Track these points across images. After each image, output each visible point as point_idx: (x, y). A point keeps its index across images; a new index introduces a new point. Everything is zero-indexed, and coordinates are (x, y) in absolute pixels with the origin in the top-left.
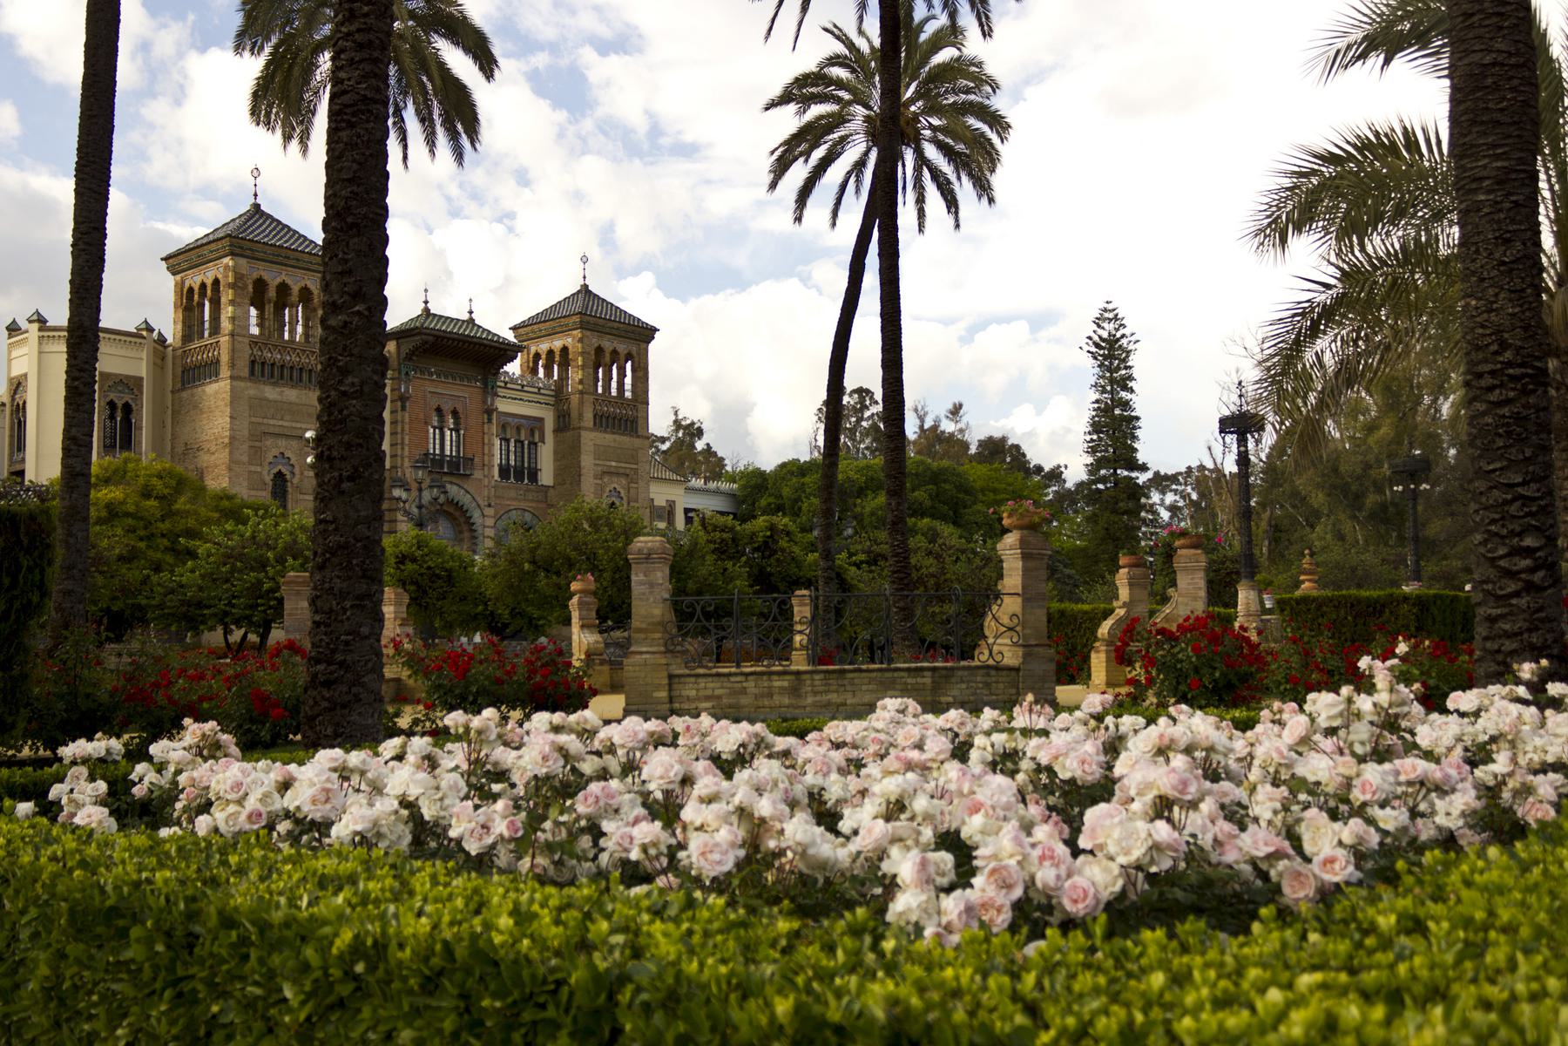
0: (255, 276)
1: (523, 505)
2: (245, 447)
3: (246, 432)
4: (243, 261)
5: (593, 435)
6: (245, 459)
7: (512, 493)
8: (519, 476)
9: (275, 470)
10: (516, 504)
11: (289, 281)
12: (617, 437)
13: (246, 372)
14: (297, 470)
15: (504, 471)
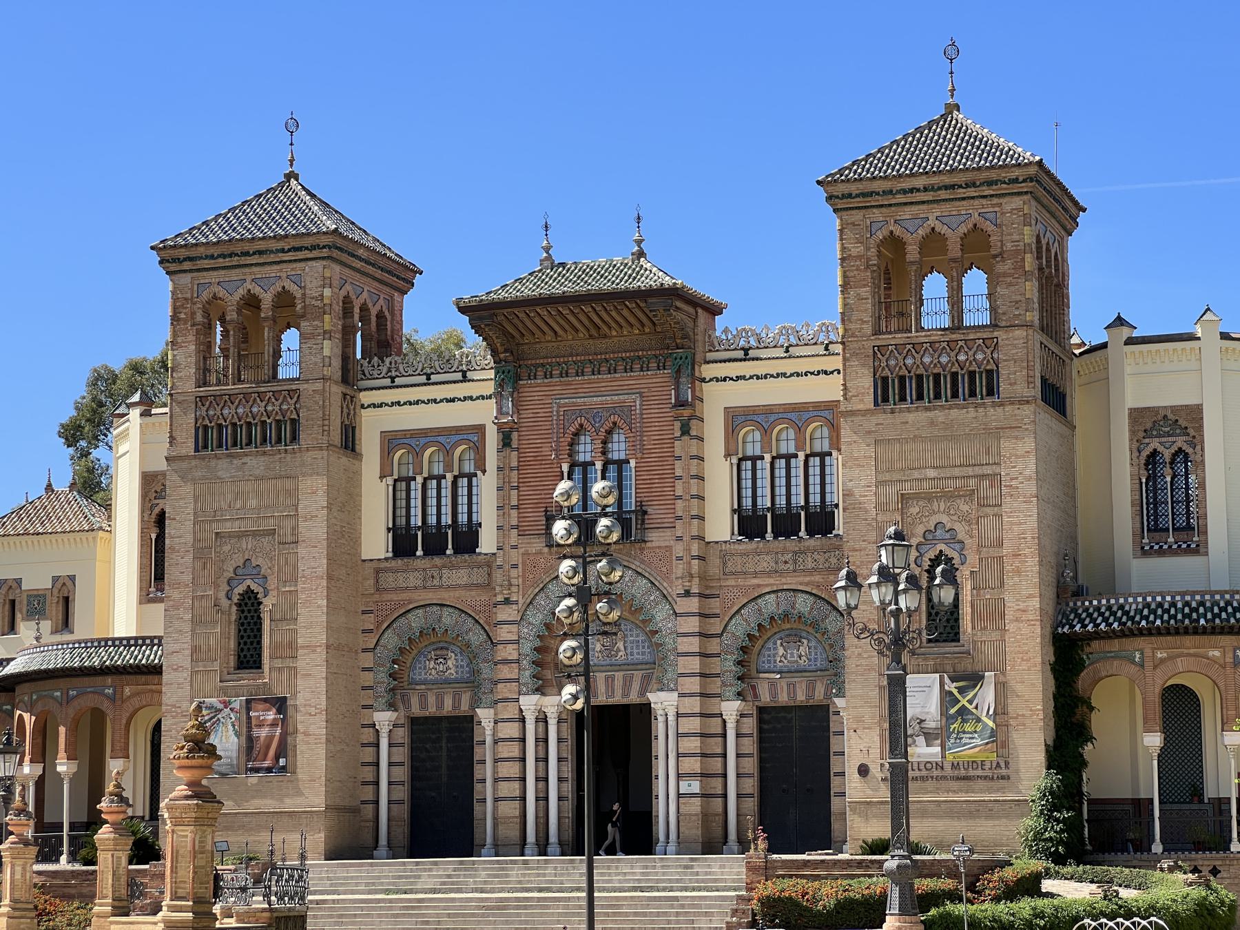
0: (206, 295)
1: (791, 582)
2: (189, 558)
3: (189, 538)
4: (186, 279)
5: (871, 422)
6: (187, 578)
7: (766, 563)
8: (786, 525)
9: (241, 589)
10: (773, 582)
11: (257, 290)
12: (939, 416)
13: (188, 448)
14: (272, 583)
15: (749, 524)
